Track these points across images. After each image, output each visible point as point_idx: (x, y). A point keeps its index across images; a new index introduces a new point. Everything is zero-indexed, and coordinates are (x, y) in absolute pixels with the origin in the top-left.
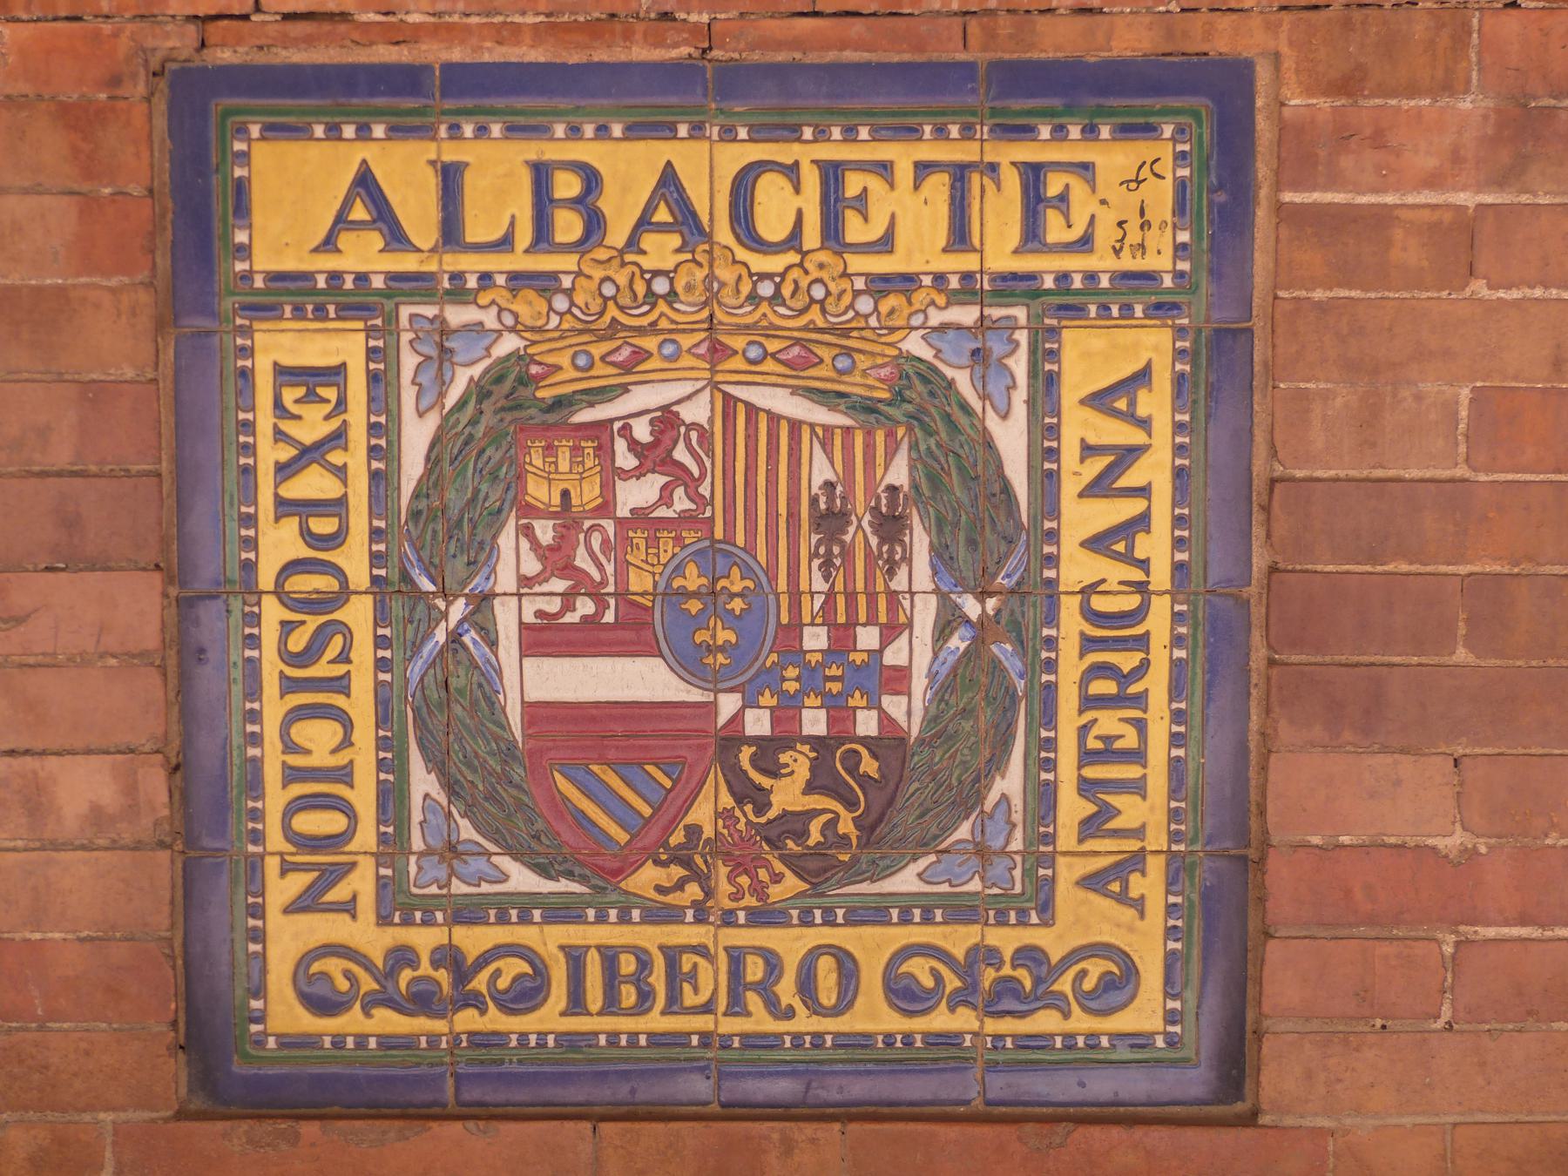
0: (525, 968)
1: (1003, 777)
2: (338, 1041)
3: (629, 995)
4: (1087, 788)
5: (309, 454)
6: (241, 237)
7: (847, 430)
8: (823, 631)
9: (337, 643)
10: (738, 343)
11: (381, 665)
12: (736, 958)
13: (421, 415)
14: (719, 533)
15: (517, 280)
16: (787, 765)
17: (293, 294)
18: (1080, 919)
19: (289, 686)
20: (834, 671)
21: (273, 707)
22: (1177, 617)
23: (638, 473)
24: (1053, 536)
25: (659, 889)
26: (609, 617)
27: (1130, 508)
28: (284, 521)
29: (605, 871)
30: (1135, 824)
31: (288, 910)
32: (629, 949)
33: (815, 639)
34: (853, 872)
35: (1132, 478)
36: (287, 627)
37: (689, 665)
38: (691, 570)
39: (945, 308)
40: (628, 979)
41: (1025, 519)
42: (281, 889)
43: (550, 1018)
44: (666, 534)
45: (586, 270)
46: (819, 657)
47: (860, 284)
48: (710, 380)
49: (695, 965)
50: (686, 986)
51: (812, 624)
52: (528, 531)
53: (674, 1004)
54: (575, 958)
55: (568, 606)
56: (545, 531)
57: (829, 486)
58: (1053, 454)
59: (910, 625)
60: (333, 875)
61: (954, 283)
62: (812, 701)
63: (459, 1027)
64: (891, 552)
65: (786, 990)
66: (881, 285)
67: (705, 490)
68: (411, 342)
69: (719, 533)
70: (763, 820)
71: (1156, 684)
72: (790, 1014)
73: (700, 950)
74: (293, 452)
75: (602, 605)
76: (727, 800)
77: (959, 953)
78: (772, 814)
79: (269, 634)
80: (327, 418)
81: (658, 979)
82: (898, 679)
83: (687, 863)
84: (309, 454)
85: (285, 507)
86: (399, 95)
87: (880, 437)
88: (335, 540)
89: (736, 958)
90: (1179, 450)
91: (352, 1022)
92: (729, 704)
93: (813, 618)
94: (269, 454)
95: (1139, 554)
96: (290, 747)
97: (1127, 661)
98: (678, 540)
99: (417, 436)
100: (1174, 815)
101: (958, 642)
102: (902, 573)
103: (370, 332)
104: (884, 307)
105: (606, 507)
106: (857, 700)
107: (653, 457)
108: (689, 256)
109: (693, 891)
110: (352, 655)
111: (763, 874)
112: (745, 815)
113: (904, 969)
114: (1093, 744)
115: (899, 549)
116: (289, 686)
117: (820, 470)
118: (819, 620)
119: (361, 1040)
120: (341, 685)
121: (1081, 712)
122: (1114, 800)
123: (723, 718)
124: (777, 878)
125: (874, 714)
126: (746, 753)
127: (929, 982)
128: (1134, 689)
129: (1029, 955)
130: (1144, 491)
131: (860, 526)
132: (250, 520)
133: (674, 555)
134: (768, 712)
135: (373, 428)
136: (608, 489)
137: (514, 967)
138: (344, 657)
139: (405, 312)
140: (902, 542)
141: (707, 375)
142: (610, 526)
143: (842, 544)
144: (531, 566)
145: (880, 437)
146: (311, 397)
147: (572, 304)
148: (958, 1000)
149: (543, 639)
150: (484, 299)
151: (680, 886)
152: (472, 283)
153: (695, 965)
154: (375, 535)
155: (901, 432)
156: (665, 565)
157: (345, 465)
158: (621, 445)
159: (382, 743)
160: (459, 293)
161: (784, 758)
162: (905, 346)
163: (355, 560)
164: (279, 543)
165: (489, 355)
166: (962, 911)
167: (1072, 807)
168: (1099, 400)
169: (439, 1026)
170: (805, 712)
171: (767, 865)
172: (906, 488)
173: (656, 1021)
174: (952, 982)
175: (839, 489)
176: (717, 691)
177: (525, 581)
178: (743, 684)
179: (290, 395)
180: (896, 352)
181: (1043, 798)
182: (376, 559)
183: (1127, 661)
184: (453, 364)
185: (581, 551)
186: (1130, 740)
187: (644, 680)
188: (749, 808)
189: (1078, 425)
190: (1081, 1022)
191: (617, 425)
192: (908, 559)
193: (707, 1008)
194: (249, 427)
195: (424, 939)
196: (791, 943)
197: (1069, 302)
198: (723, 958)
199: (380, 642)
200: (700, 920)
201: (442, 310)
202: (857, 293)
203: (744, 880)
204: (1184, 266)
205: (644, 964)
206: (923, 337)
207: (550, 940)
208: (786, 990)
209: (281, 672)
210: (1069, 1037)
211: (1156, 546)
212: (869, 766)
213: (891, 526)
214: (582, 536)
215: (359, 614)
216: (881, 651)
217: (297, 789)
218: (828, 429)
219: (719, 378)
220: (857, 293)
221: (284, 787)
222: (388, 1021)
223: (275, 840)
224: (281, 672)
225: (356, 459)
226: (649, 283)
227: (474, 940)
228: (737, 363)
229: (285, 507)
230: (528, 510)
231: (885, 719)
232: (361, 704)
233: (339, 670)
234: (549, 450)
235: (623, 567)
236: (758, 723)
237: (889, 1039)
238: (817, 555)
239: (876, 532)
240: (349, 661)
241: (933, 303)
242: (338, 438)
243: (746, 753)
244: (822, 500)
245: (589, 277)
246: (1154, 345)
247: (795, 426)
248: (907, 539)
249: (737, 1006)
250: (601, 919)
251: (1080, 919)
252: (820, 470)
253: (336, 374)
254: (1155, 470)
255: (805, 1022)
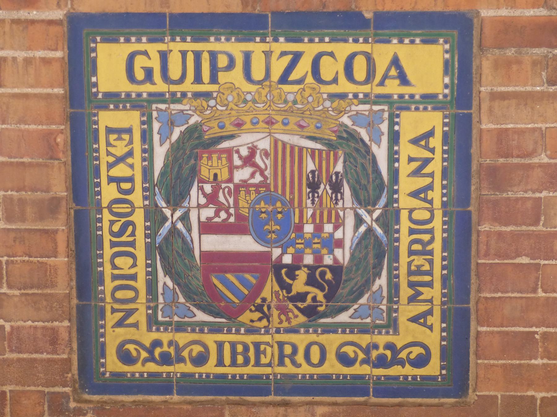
0: (202, 349)
1: (379, 279)
2: (133, 374)
3: (240, 359)
4: (411, 285)
5: (120, 160)
6: (94, 79)
7: (320, 151)
8: (312, 226)
9: (130, 228)
10: (279, 118)
11: (146, 236)
12: (281, 345)
13: (161, 145)
14: (272, 190)
15: (197, 95)
16: (298, 275)
17: (114, 100)
18: (408, 332)
19: (113, 245)
20: (316, 240)
21: (108, 252)
22: (444, 223)
23: (242, 167)
24: (397, 192)
25: (252, 321)
26: (232, 220)
27: (428, 180)
28: (111, 184)
29: (232, 314)
30: (429, 297)
31: (112, 327)
32: (240, 343)
33: (309, 228)
34: (324, 315)
35: (427, 170)
36: (112, 223)
37: (261, 237)
38: (262, 203)
39: (357, 106)
40: (240, 354)
41: (386, 184)
42: (111, 319)
43: (210, 367)
44: (253, 189)
45: (221, 90)
46: (310, 235)
47: (325, 96)
48: (270, 133)
49: (265, 349)
50: (262, 356)
51: (307, 223)
52: (201, 189)
53: (258, 363)
54: (220, 345)
55: (217, 214)
56: (208, 188)
57: (313, 172)
58: (398, 160)
59: (343, 224)
60: (130, 313)
61: (361, 96)
62: (308, 251)
63: (178, 370)
64: (336, 196)
65: (300, 358)
66: (332, 97)
67: (267, 173)
68: (156, 118)
69: (272, 190)
70: (290, 295)
71: (437, 246)
72: (299, 366)
73: (267, 344)
74: (114, 159)
75: (229, 215)
76: (277, 288)
77: (364, 346)
78: (294, 292)
79: (106, 225)
80: (126, 146)
81: (252, 353)
82: (340, 244)
83: (263, 312)
84: (120, 160)
85: (111, 180)
86: (153, 24)
87: (332, 153)
88: (130, 192)
89: (281, 345)
90: (444, 160)
91: (138, 368)
92: (276, 252)
93: (307, 221)
94: (105, 159)
95: (429, 198)
96: (114, 267)
97: (426, 237)
98: (257, 192)
99: (160, 154)
100: (444, 295)
101: (363, 229)
102: (340, 203)
103: (143, 115)
104: (335, 104)
105: (230, 180)
106: (324, 251)
107: (249, 161)
108: (261, 86)
109: (264, 322)
110: (136, 233)
111: (290, 315)
112: (282, 292)
113: (342, 351)
114: (413, 268)
115: (339, 195)
116: (113, 245)
117: (310, 166)
118: (310, 221)
119: (142, 374)
120: (132, 244)
121: (409, 257)
122: (421, 289)
123: (274, 257)
124: (296, 316)
125: (331, 256)
126: (283, 271)
127: (352, 355)
128: (429, 248)
129: (390, 346)
130: (432, 175)
131: (325, 188)
132: (99, 185)
133: (256, 196)
134: (291, 255)
135: (144, 151)
136: (231, 173)
137: (197, 349)
138: (133, 234)
139: (154, 106)
140: (341, 193)
141: (268, 130)
142: (231, 186)
143: (318, 193)
144: (203, 201)
145: (332, 153)
146: (120, 139)
147: (217, 103)
148: (364, 362)
149: (207, 228)
150: (185, 101)
151: (260, 319)
152: (179, 95)
153: (265, 349)
154: (144, 189)
155: (340, 152)
156: (252, 201)
157: (133, 164)
158: (236, 156)
159: (147, 266)
160: (174, 98)
161: (297, 272)
162: (341, 120)
163: (137, 198)
164: (109, 192)
165: (188, 123)
166: (364, 330)
167: (405, 292)
168: (415, 141)
169: (170, 369)
170: (305, 256)
171: (291, 311)
172: (342, 172)
173: (250, 370)
174: (361, 356)
175: (317, 173)
176: (272, 248)
177: (199, 206)
178: (282, 245)
179: (112, 137)
180: (338, 123)
181: (394, 288)
182: (145, 198)
183: (426, 237)
184: (174, 126)
185: (221, 194)
186: (427, 267)
187: (245, 243)
188: (284, 291)
189: (406, 150)
190: (409, 370)
191: (235, 149)
192: (342, 198)
193: (269, 365)
194: (97, 150)
195: (165, 337)
196: (301, 340)
197: (402, 104)
198: (276, 346)
199: (146, 228)
200: (267, 332)
201: (169, 106)
202: (324, 100)
203: (283, 317)
204: (447, 91)
205: (246, 348)
206: (348, 117)
207: (210, 339)
208: (300, 358)
209: (110, 240)
210: (406, 377)
211: (436, 195)
212: (329, 276)
213: (336, 188)
214: (221, 191)
215: (138, 218)
216: (333, 233)
217: (118, 283)
218: (313, 151)
219: (272, 131)
220: (324, 100)
221: (112, 282)
222: (152, 367)
223: (109, 299)
224: (110, 240)
225: (137, 160)
226: (245, 96)
227: (182, 338)
228: (278, 126)
229: (111, 180)
230: (202, 181)
231: (335, 260)
232: (140, 252)
233: (131, 239)
234: (210, 158)
235: (236, 202)
236: (287, 259)
237: (338, 376)
238: (309, 198)
239: (330, 189)
240: (135, 236)
241: (353, 104)
242: (130, 154)
243: (283, 271)
244: (310, 176)
245: (224, 94)
246: (434, 120)
247: (301, 149)
248: (342, 191)
249: (281, 363)
250: (229, 332)
251: (408, 332)
252: (310, 166)
253: (129, 131)
254: (436, 166)
255: (306, 369)
